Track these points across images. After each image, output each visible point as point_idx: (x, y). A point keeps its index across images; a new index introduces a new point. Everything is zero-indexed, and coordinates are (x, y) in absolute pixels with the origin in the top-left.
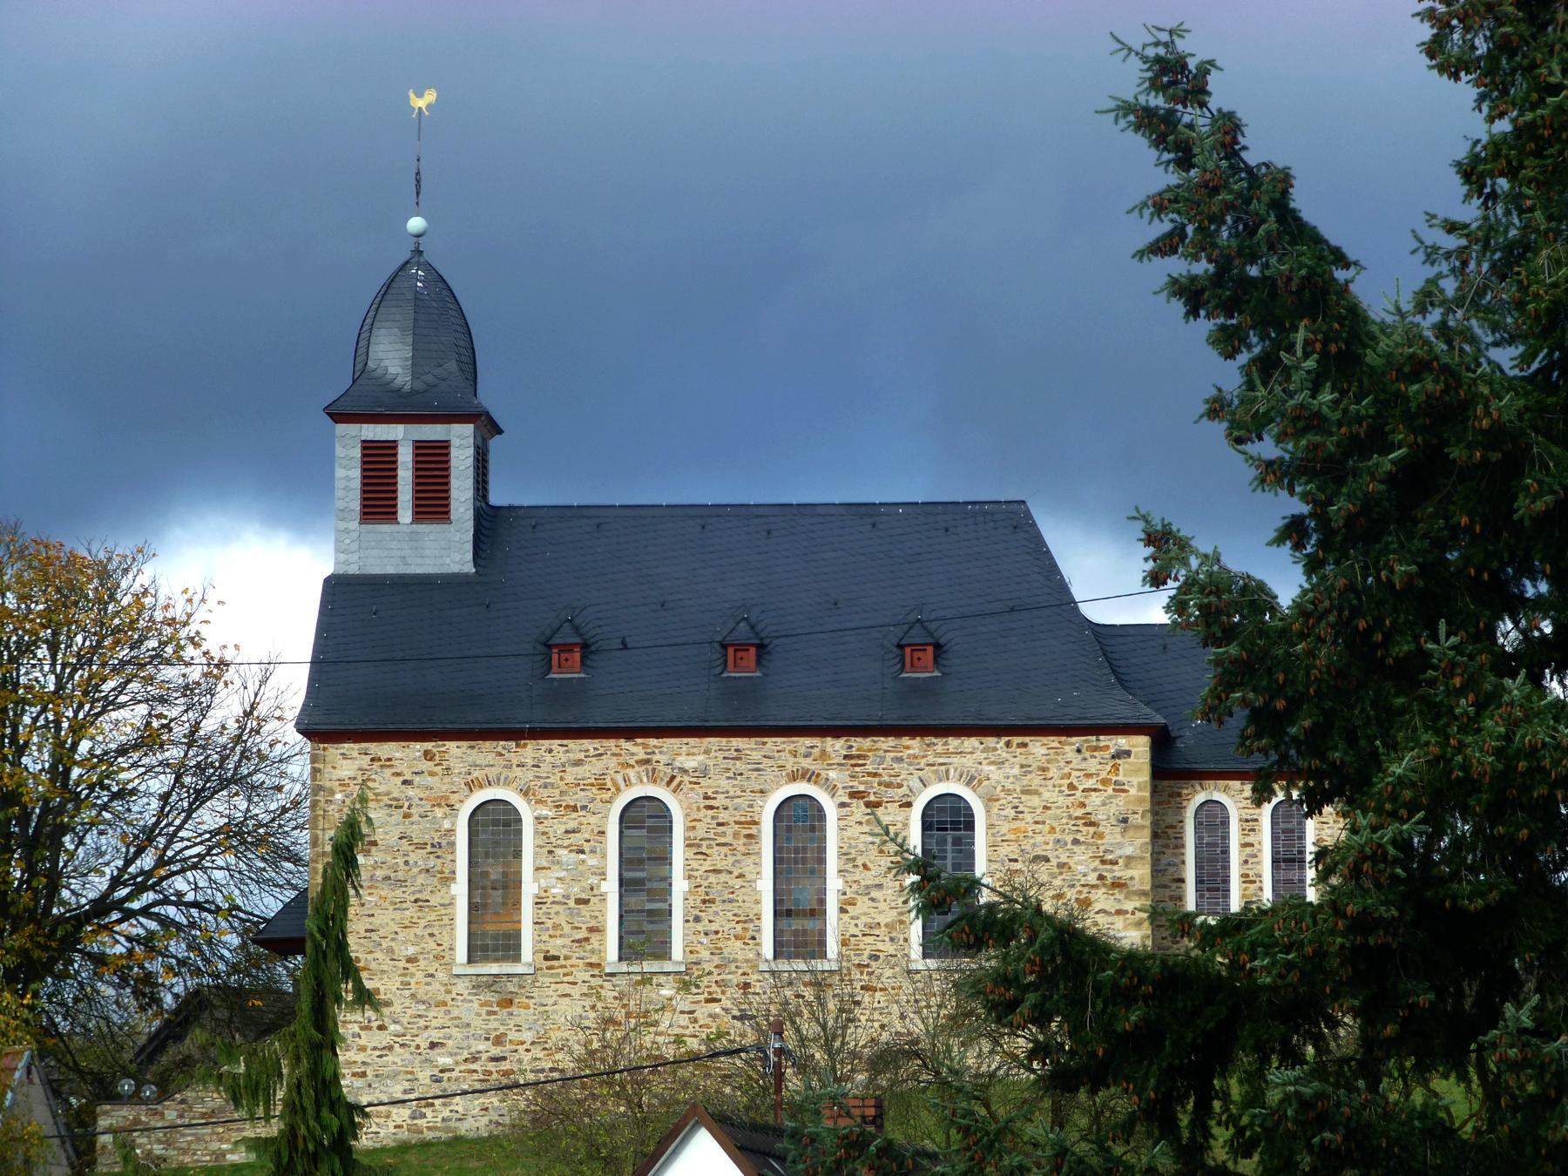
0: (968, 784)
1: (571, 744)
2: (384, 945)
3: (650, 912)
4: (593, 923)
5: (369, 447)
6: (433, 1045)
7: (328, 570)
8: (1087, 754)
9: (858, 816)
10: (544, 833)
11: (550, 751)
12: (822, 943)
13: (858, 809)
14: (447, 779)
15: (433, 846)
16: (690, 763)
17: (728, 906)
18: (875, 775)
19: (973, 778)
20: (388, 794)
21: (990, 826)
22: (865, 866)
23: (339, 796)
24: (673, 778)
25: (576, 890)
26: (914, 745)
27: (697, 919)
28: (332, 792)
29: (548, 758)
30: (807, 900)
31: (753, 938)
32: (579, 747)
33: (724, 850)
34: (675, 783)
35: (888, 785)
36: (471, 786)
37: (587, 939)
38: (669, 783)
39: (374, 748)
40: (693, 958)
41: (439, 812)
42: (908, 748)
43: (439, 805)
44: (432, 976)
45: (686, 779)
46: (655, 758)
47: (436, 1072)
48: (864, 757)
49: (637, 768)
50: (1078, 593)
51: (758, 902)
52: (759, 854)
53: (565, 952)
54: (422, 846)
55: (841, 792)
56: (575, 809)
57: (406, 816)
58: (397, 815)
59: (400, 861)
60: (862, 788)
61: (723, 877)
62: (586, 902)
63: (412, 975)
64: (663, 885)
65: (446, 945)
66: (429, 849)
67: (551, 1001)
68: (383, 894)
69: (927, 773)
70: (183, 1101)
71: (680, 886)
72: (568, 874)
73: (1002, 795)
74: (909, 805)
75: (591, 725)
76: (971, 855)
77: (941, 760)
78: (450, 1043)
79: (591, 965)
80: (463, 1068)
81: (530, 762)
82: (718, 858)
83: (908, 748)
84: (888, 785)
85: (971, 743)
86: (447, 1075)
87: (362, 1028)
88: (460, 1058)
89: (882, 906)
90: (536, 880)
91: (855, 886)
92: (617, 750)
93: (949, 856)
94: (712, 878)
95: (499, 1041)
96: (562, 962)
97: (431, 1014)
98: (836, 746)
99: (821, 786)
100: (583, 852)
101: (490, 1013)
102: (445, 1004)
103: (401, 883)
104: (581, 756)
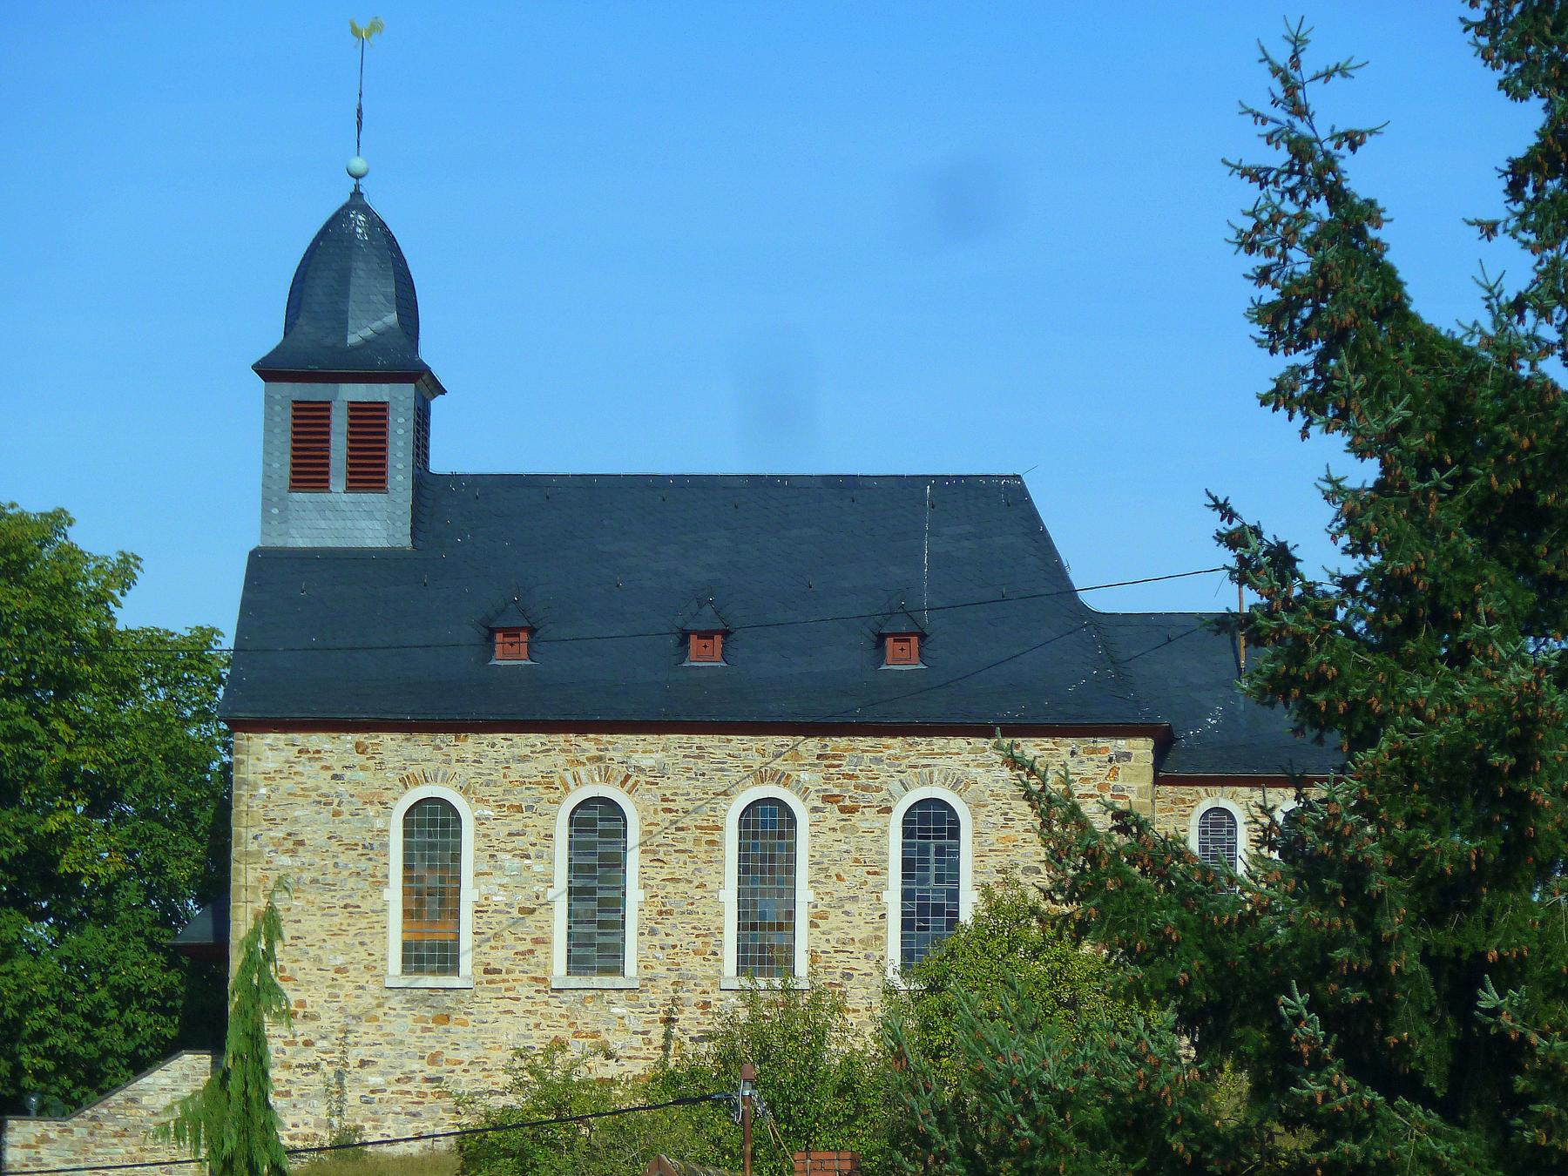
0: (953, 788)
1: (515, 737)
2: (312, 954)
3: (601, 924)
4: (539, 934)
5: (299, 407)
6: (363, 1064)
7: (255, 542)
8: (1085, 757)
9: (831, 823)
10: (485, 836)
11: (493, 746)
12: (790, 961)
13: (832, 814)
14: (380, 775)
15: (364, 847)
16: (647, 762)
17: (688, 918)
18: (851, 777)
19: (958, 781)
20: (317, 789)
21: (977, 834)
22: (838, 877)
23: (263, 791)
24: (628, 777)
25: (520, 899)
26: (896, 744)
27: (653, 932)
28: (255, 786)
29: (491, 753)
30: (774, 914)
31: (715, 954)
32: (525, 742)
33: (684, 857)
34: (630, 782)
35: (866, 788)
36: (406, 782)
37: (531, 952)
38: (623, 784)
39: (300, 738)
40: (649, 973)
41: (371, 811)
42: (887, 747)
43: (371, 803)
44: (361, 988)
45: (642, 778)
46: (609, 755)
47: (366, 1092)
48: (840, 757)
49: (588, 766)
50: (1077, 579)
51: (719, 914)
52: (722, 862)
53: (507, 964)
54: (352, 847)
55: (813, 795)
56: (519, 809)
57: (336, 814)
58: (326, 813)
59: (330, 862)
60: (836, 791)
61: (682, 887)
62: (532, 911)
63: (341, 987)
64: (616, 894)
65: (378, 956)
66: (360, 850)
67: (491, 1018)
68: (311, 898)
69: (909, 775)
70: (94, 1118)
71: (634, 895)
72: (513, 877)
73: (990, 800)
74: (888, 810)
75: (538, 717)
76: (955, 866)
77: (925, 762)
78: (381, 1061)
79: (535, 979)
80: (395, 1088)
81: (471, 757)
82: (676, 865)
83: (887, 747)
84: (866, 788)
85: (958, 743)
86: (378, 1096)
87: (286, 1043)
88: (392, 1078)
89: (857, 920)
90: (476, 886)
91: (827, 898)
92: (566, 746)
93: (933, 866)
94: (670, 887)
95: (434, 1060)
96: (504, 976)
97: (361, 1030)
98: (811, 745)
99: (791, 789)
100: (528, 857)
101: (425, 1030)
102: (376, 1019)
103: (329, 886)
104: (527, 751)
